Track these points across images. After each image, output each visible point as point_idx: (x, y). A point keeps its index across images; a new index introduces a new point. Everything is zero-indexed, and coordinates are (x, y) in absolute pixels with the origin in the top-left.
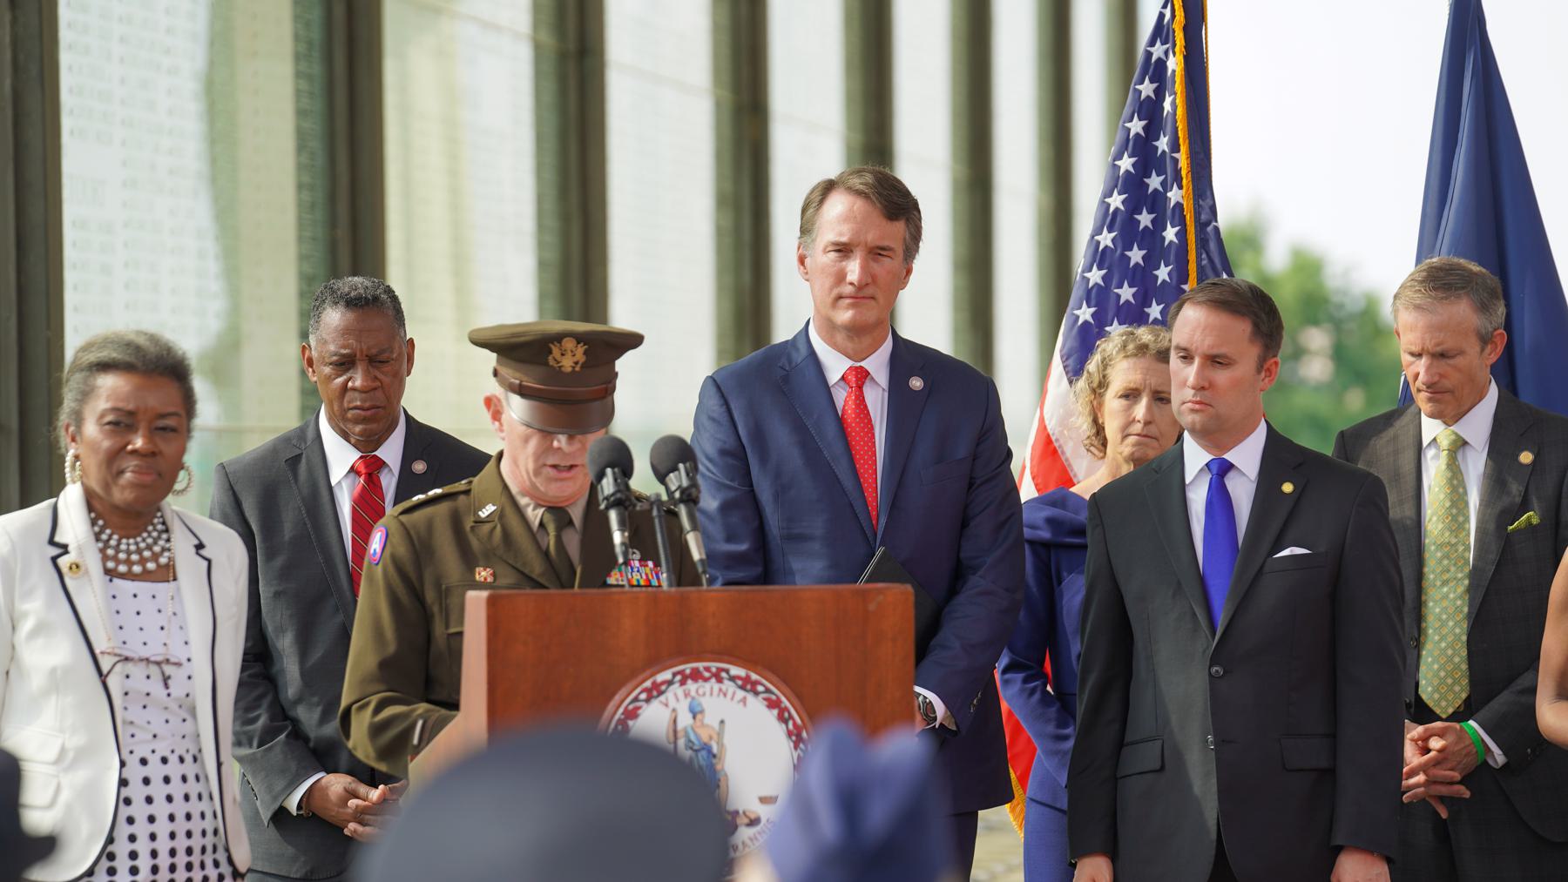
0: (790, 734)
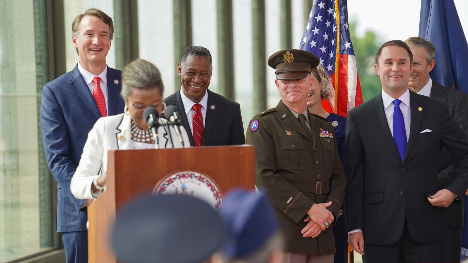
0: (215, 195)
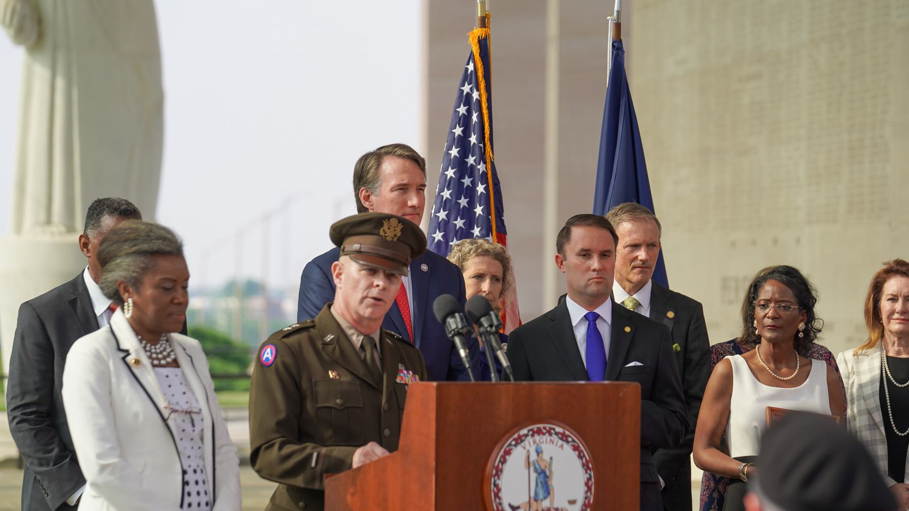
0: (583, 465)
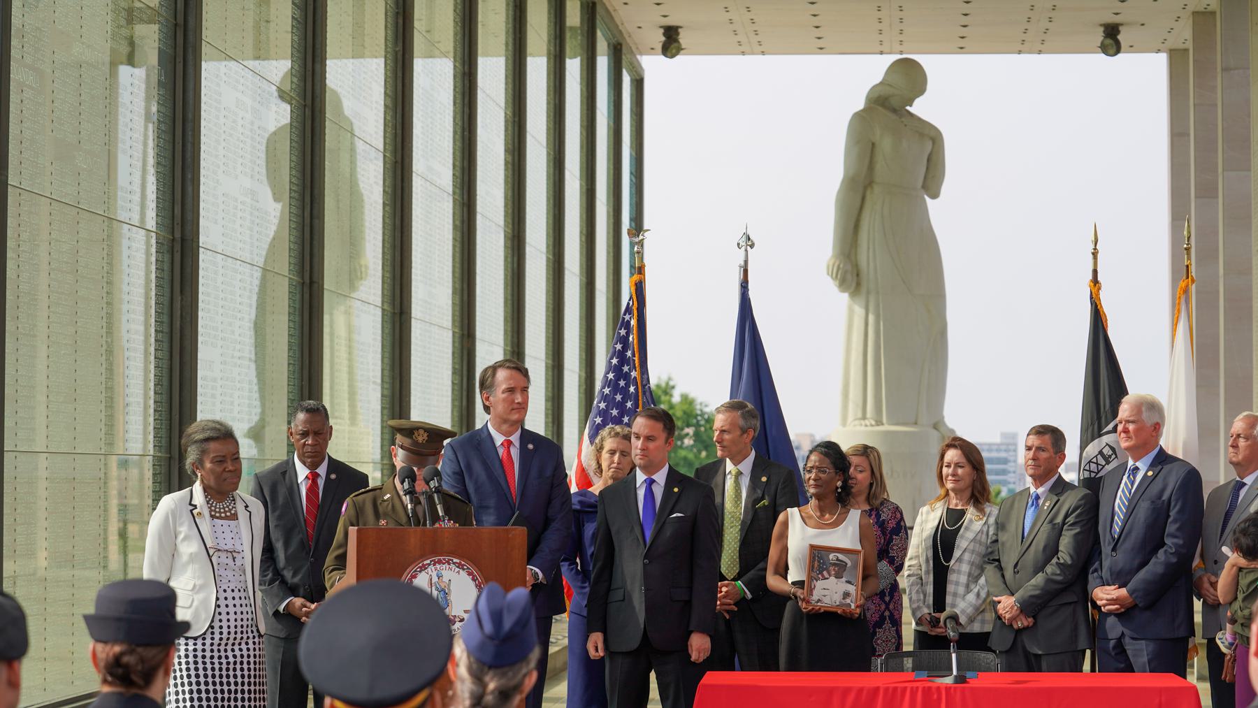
0: (476, 586)
